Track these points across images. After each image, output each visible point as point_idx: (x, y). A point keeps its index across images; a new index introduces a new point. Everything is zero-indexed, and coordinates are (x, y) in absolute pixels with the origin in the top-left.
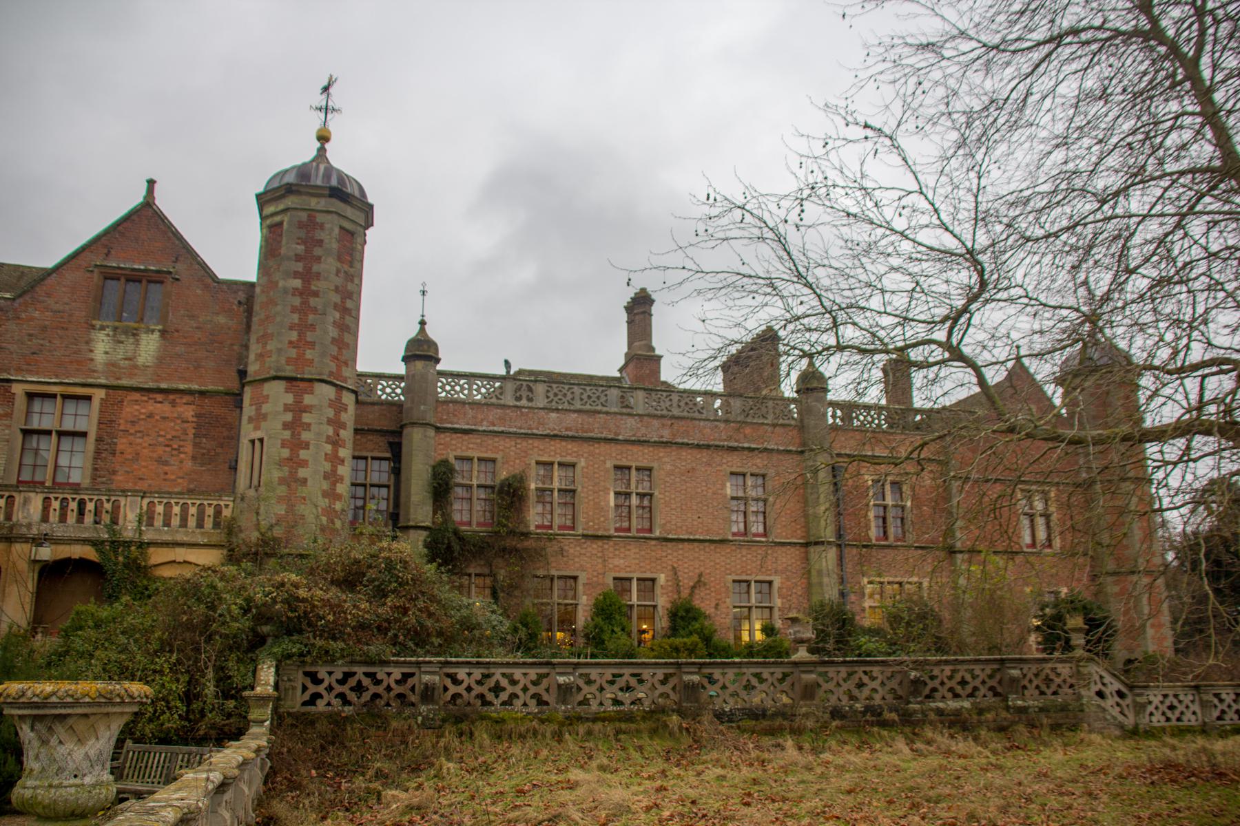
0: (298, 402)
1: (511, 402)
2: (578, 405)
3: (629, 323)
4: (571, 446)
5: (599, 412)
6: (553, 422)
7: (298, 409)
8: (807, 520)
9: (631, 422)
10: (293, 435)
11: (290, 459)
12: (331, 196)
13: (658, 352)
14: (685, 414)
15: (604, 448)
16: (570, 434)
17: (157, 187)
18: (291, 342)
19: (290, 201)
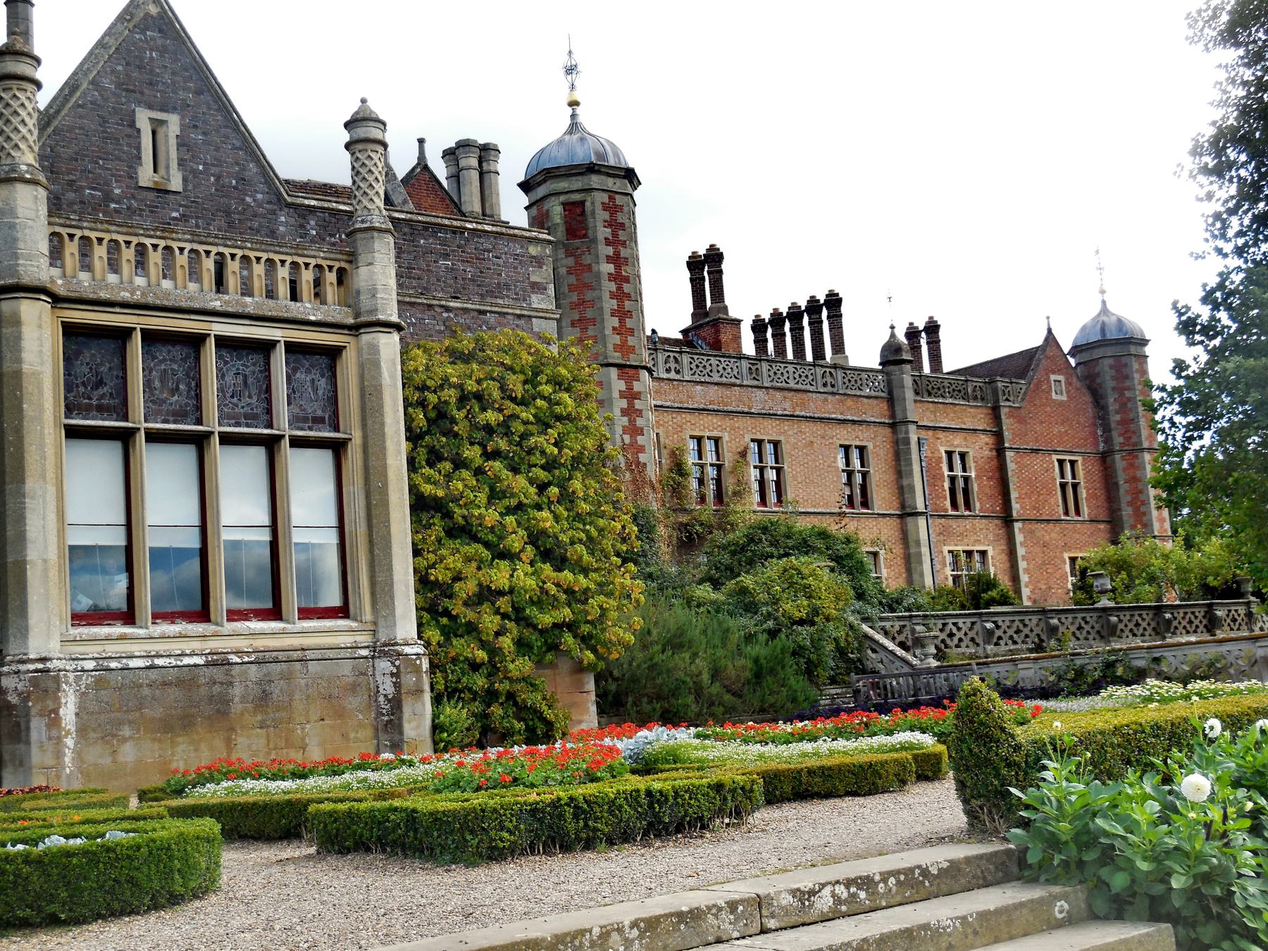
0: (630, 388)
1: (665, 376)
2: (716, 378)
3: (692, 280)
4: (715, 420)
5: (734, 385)
6: (700, 396)
7: (630, 395)
8: (902, 491)
9: (760, 394)
10: (630, 421)
11: (631, 445)
12: (624, 177)
13: (733, 313)
14: (799, 386)
15: (741, 422)
16: (716, 407)
17: (426, 145)
18: (614, 329)
19: (595, 180)
